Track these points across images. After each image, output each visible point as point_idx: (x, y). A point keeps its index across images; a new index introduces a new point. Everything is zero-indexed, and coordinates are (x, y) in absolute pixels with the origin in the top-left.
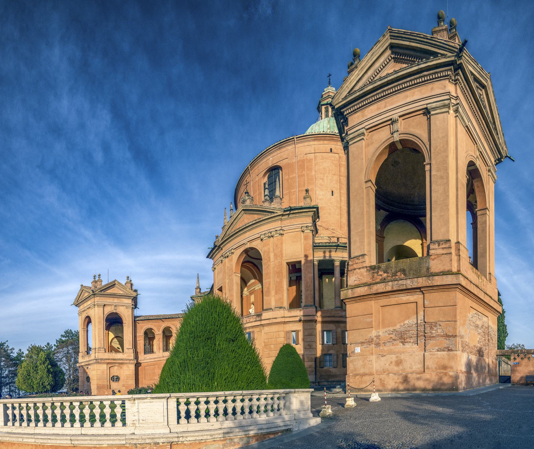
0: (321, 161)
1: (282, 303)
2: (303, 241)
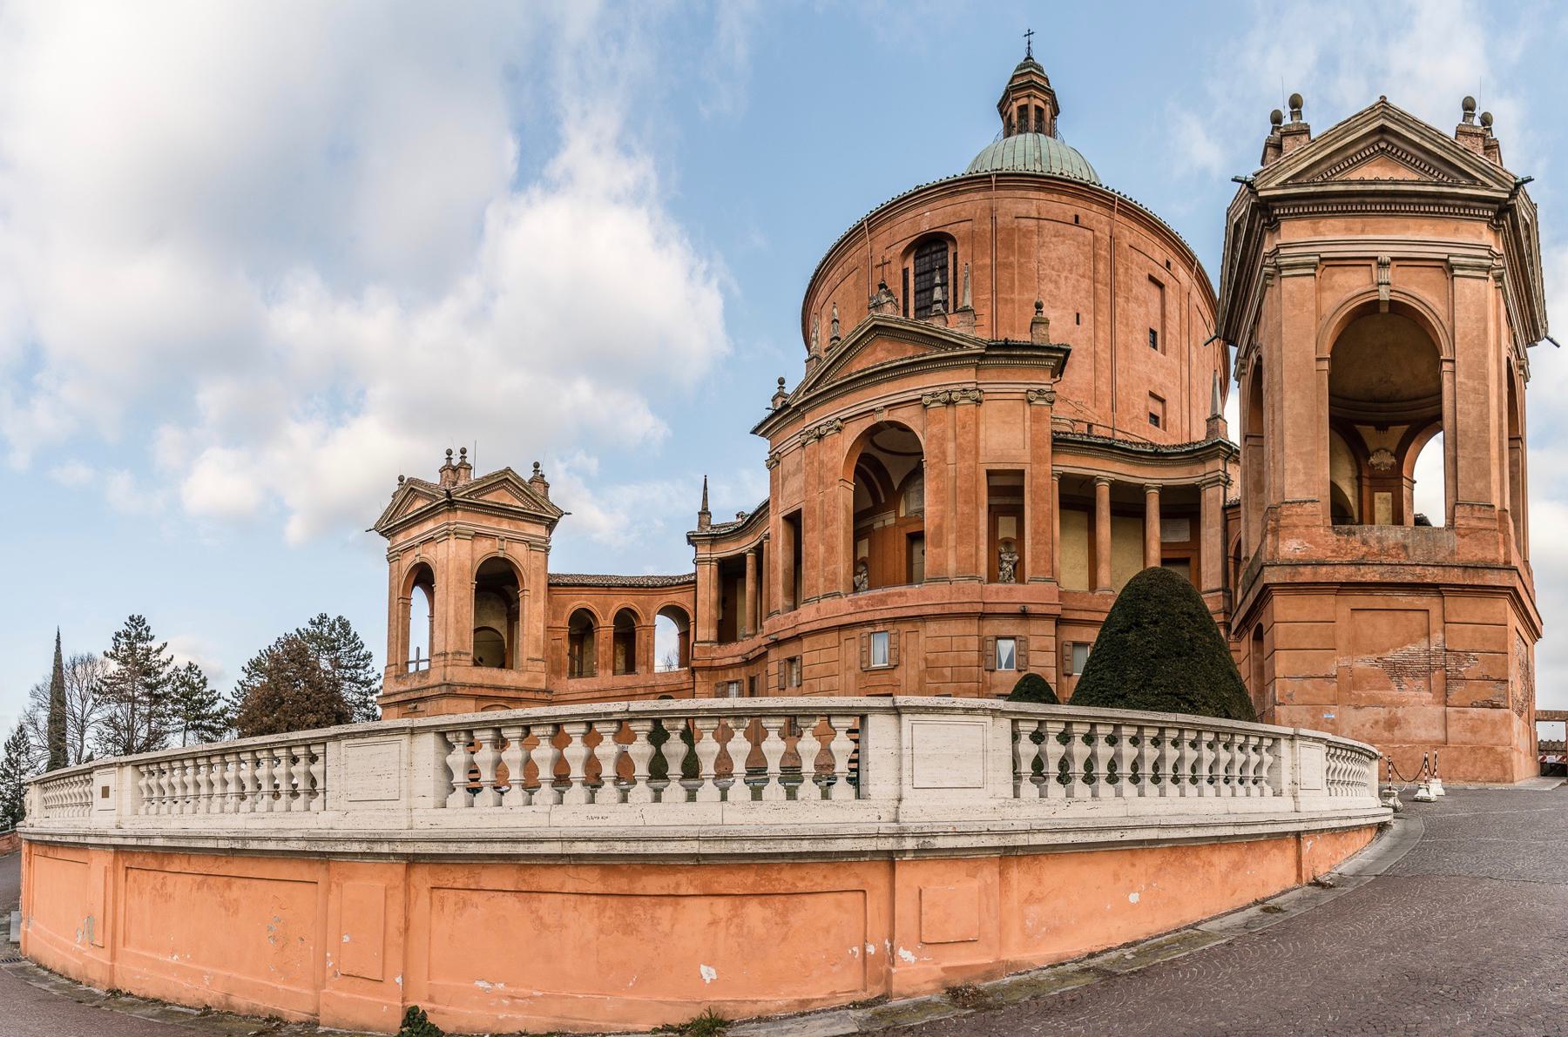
0: (1054, 239)
1: (977, 570)
2: (1028, 423)
